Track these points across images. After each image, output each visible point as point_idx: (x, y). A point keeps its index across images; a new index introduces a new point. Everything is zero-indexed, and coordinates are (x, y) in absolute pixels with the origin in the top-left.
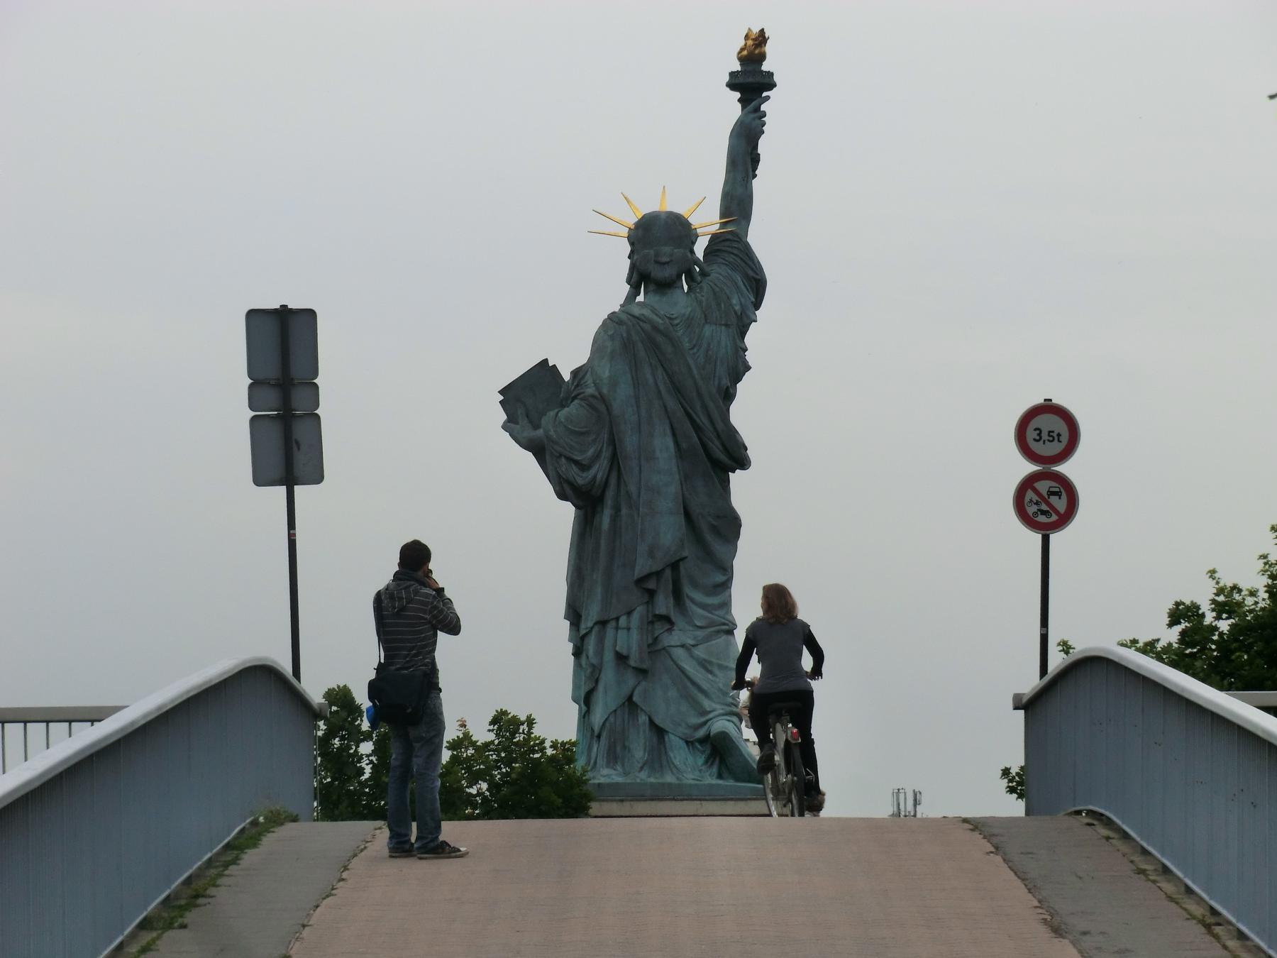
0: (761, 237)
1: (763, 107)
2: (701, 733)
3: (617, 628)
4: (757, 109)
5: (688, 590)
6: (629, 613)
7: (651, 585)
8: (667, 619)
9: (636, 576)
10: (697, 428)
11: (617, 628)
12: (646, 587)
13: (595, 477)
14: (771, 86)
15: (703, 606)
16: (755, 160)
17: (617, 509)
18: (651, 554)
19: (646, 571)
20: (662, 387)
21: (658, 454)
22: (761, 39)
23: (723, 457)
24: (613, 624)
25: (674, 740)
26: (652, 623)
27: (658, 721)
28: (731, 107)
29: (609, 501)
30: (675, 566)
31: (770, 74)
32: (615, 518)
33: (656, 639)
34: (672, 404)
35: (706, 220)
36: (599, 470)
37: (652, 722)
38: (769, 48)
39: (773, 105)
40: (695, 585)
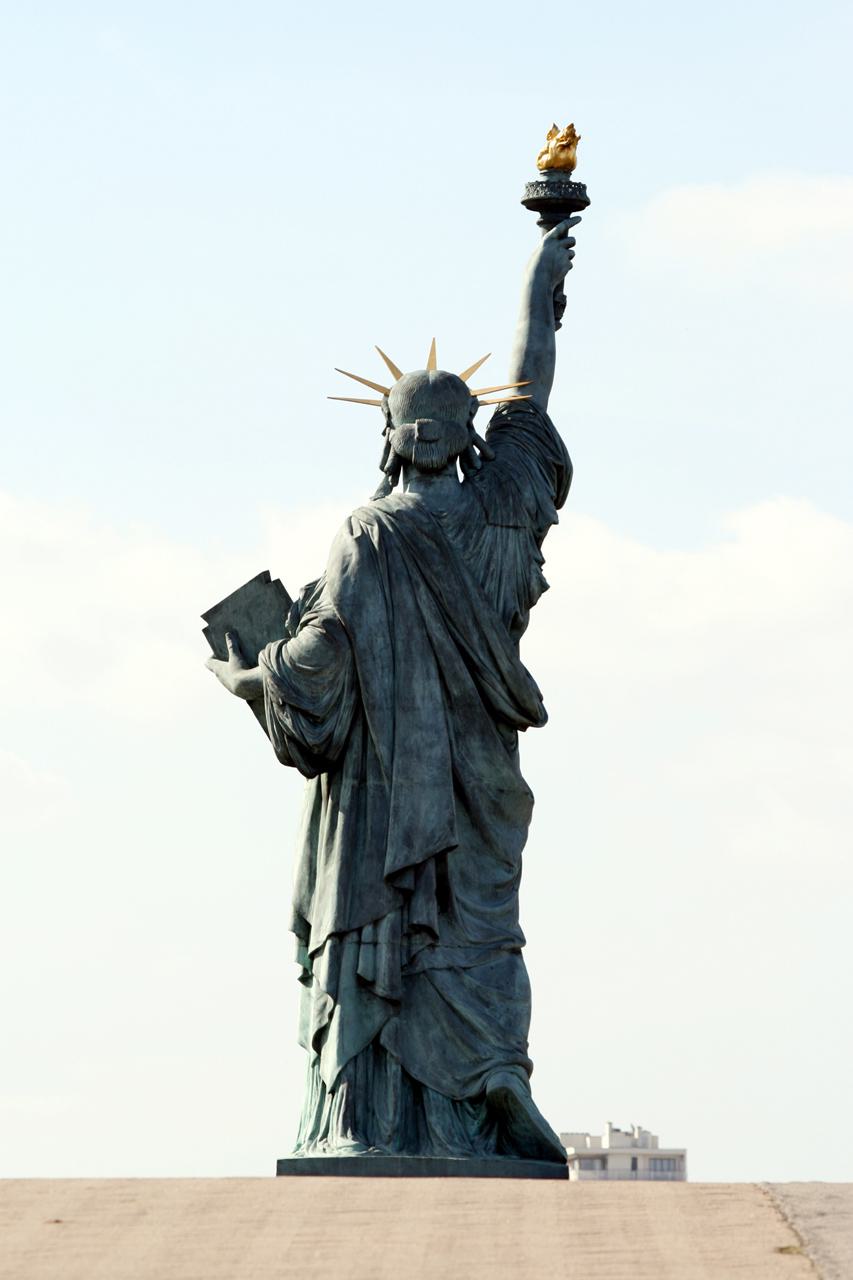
1: (572, 232)
2: (474, 1090)
3: (359, 943)
4: (563, 235)
5: (457, 891)
6: (376, 923)
7: (408, 882)
8: (428, 930)
9: (386, 873)
10: (474, 669)
11: (359, 943)
12: (402, 885)
13: (331, 735)
14: (582, 202)
15: (481, 916)
16: (560, 305)
17: (362, 778)
18: (408, 841)
19: (399, 865)
20: (426, 613)
21: (419, 702)
22: (572, 138)
23: (512, 712)
24: (354, 936)
25: (433, 1099)
26: (408, 936)
27: (415, 1073)
30: (440, 858)
31: (581, 188)
33: (412, 960)
34: (438, 633)
35: (494, 384)
36: (339, 725)
37: (406, 1075)
38: (581, 153)
39: (585, 230)
40: (466, 881)
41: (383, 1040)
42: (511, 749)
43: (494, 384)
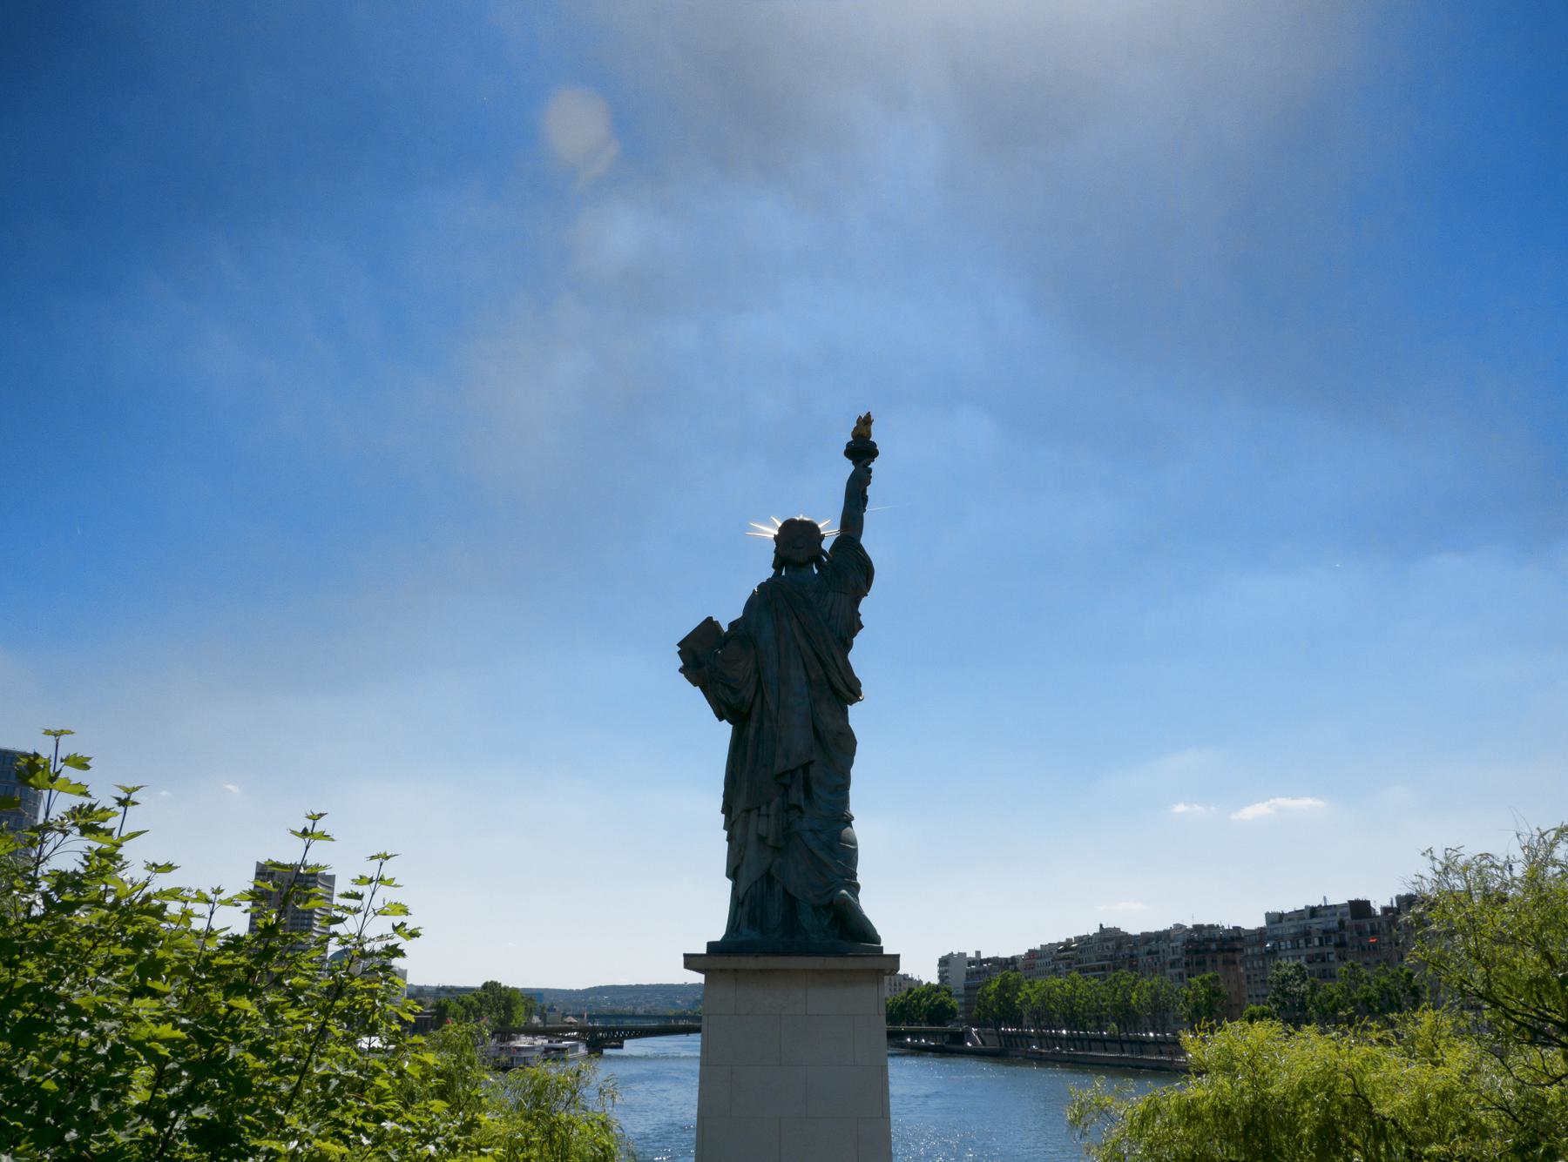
0: (871, 541)
5: (815, 788)
6: (768, 803)
7: (787, 780)
8: (798, 807)
16: (865, 499)
22: (865, 422)
23: (842, 688)
27: (791, 891)
28: (848, 467)
29: (754, 717)
30: (806, 767)
32: (759, 730)
33: (790, 824)
34: (803, 643)
35: (829, 529)
37: (786, 892)
38: (874, 428)
41: (773, 871)
42: (845, 712)
43: (829, 529)
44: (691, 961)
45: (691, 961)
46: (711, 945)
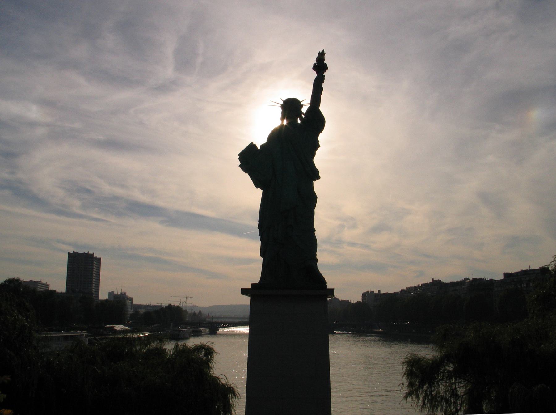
0: (323, 108)
16: (322, 89)
28: (314, 75)
38: (326, 56)
44: (244, 292)
45: (244, 292)
46: (253, 285)
